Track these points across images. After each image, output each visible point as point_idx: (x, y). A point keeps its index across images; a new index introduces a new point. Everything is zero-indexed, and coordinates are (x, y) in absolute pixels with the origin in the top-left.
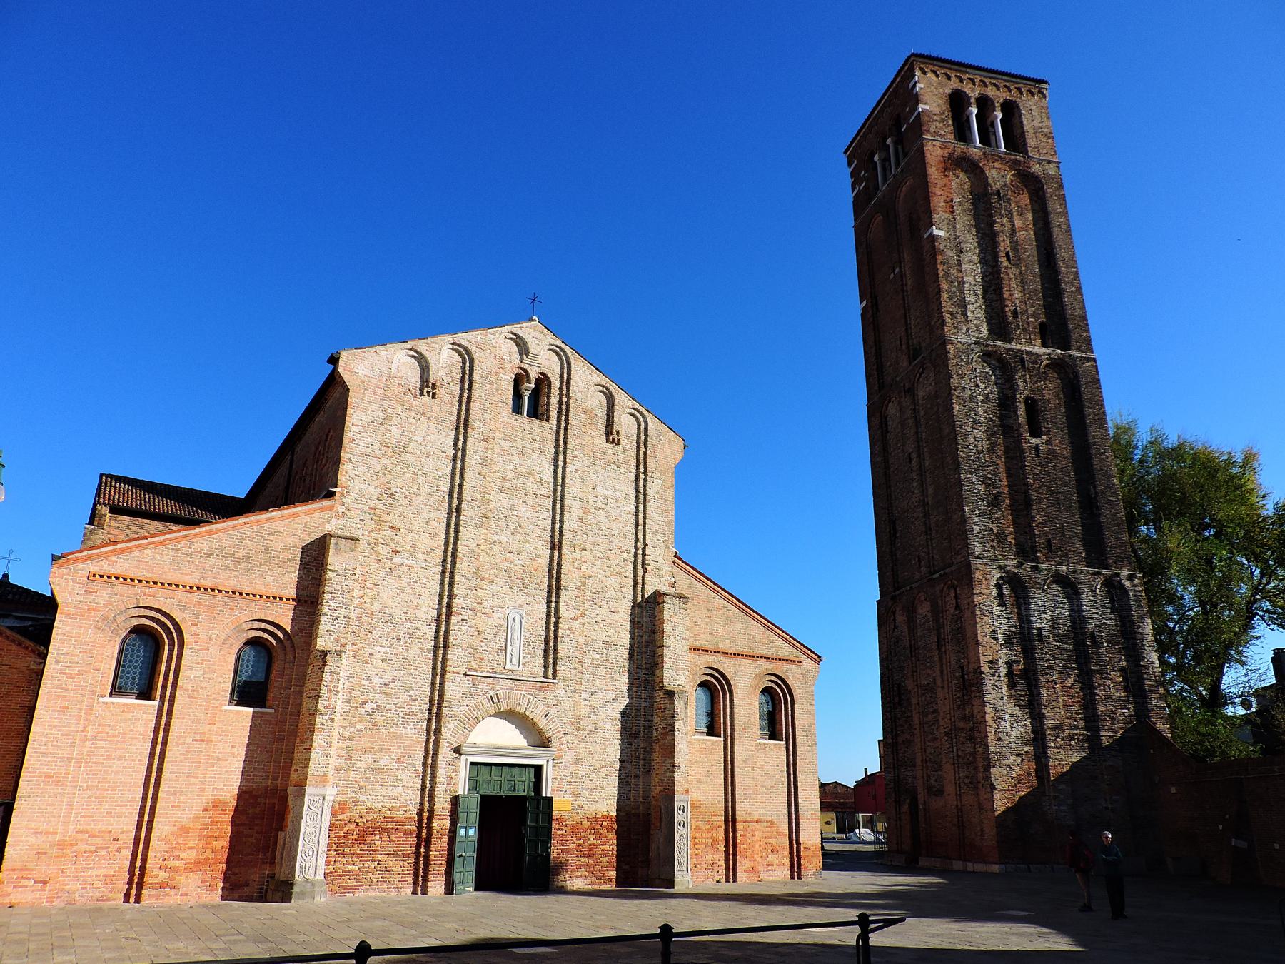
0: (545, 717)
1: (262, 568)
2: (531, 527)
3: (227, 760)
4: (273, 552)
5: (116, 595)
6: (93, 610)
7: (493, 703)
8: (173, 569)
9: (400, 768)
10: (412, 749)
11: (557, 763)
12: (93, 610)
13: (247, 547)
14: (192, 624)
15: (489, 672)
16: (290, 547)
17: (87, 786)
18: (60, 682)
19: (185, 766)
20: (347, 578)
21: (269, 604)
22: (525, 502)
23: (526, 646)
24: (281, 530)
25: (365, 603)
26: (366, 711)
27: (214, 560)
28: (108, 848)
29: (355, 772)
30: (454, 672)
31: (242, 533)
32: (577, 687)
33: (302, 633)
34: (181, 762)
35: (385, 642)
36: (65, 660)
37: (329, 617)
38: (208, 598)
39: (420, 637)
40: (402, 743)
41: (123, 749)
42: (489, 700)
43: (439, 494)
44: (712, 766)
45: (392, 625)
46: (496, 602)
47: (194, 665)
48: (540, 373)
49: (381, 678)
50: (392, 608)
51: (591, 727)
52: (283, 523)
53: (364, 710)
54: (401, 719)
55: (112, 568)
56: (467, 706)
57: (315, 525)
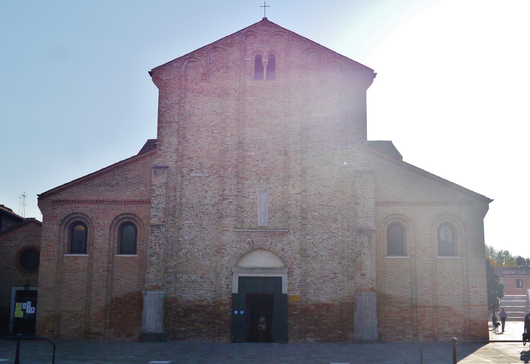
0: (282, 251)
1: (124, 188)
2: (269, 144)
3: (119, 279)
4: (129, 180)
5: (64, 209)
6: (56, 217)
7: (250, 245)
8: (86, 194)
9: (203, 280)
10: (208, 271)
11: (290, 276)
12: (56, 217)
13: (117, 179)
14: (96, 219)
15: (248, 229)
16: (137, 176)
17: (64, 292)
18: (47, 249)
19: (100, 282)
20: (162, 188)
21: (129, 206)
22: (265, 130)
23: (270, 212)
24: (132, 168)
25: (177, 199)
26: (183, 253)
27: (103, 187)
28: (75, 318)
29: (180, 283)
30: (226, 230)
31: (114, 173)
32: (303, 233)
33: (146, 217)
34: (98, 281)
35: (189, 218)
36: (48, 239)
37: (155, 208)
38: (102, 206)
39: (209, 213)
40: (202, 268)
41: (76, 276)
42: (247, 243)
43: (214, 135)
44: (400, 274)
45: (193, 209)
46: (251, 190)
47: (99, 237)
48: (272, 51)
49: (189, 236)
50: (192, 200)
51: (314, 254)
52: (132, 165)
53: (181, 253)
54: (201, 257)
55: (61, 197)
56: (235, 247)
57: (148, 163)
